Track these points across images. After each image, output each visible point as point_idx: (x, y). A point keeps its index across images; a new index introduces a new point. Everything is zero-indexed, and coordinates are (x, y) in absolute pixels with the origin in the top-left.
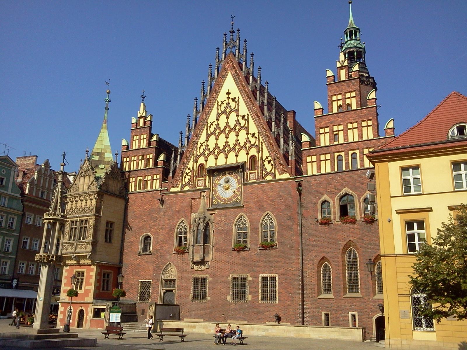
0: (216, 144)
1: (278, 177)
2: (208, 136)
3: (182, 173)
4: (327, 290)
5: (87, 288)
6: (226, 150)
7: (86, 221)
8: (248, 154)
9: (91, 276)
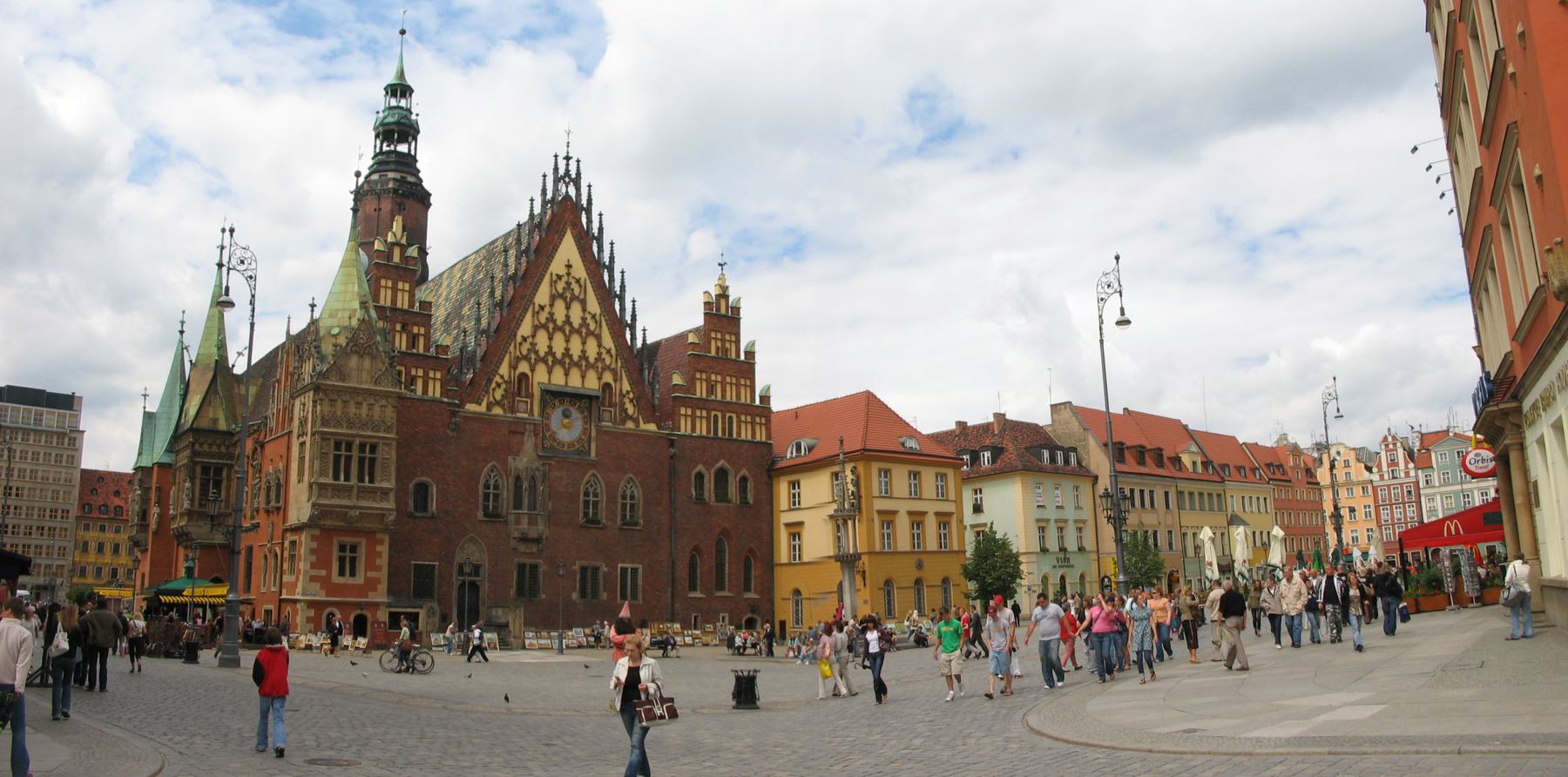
0: (550, 347)
1: (643, 426)
2: (536, 328)
3: (490, 381)
4: (693, 588)
5: (371, 574)
6: (567, 362)
7: (373, 448)
8: (600, 379)
9: (379, 554)
